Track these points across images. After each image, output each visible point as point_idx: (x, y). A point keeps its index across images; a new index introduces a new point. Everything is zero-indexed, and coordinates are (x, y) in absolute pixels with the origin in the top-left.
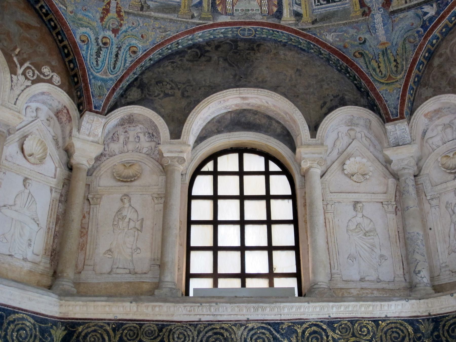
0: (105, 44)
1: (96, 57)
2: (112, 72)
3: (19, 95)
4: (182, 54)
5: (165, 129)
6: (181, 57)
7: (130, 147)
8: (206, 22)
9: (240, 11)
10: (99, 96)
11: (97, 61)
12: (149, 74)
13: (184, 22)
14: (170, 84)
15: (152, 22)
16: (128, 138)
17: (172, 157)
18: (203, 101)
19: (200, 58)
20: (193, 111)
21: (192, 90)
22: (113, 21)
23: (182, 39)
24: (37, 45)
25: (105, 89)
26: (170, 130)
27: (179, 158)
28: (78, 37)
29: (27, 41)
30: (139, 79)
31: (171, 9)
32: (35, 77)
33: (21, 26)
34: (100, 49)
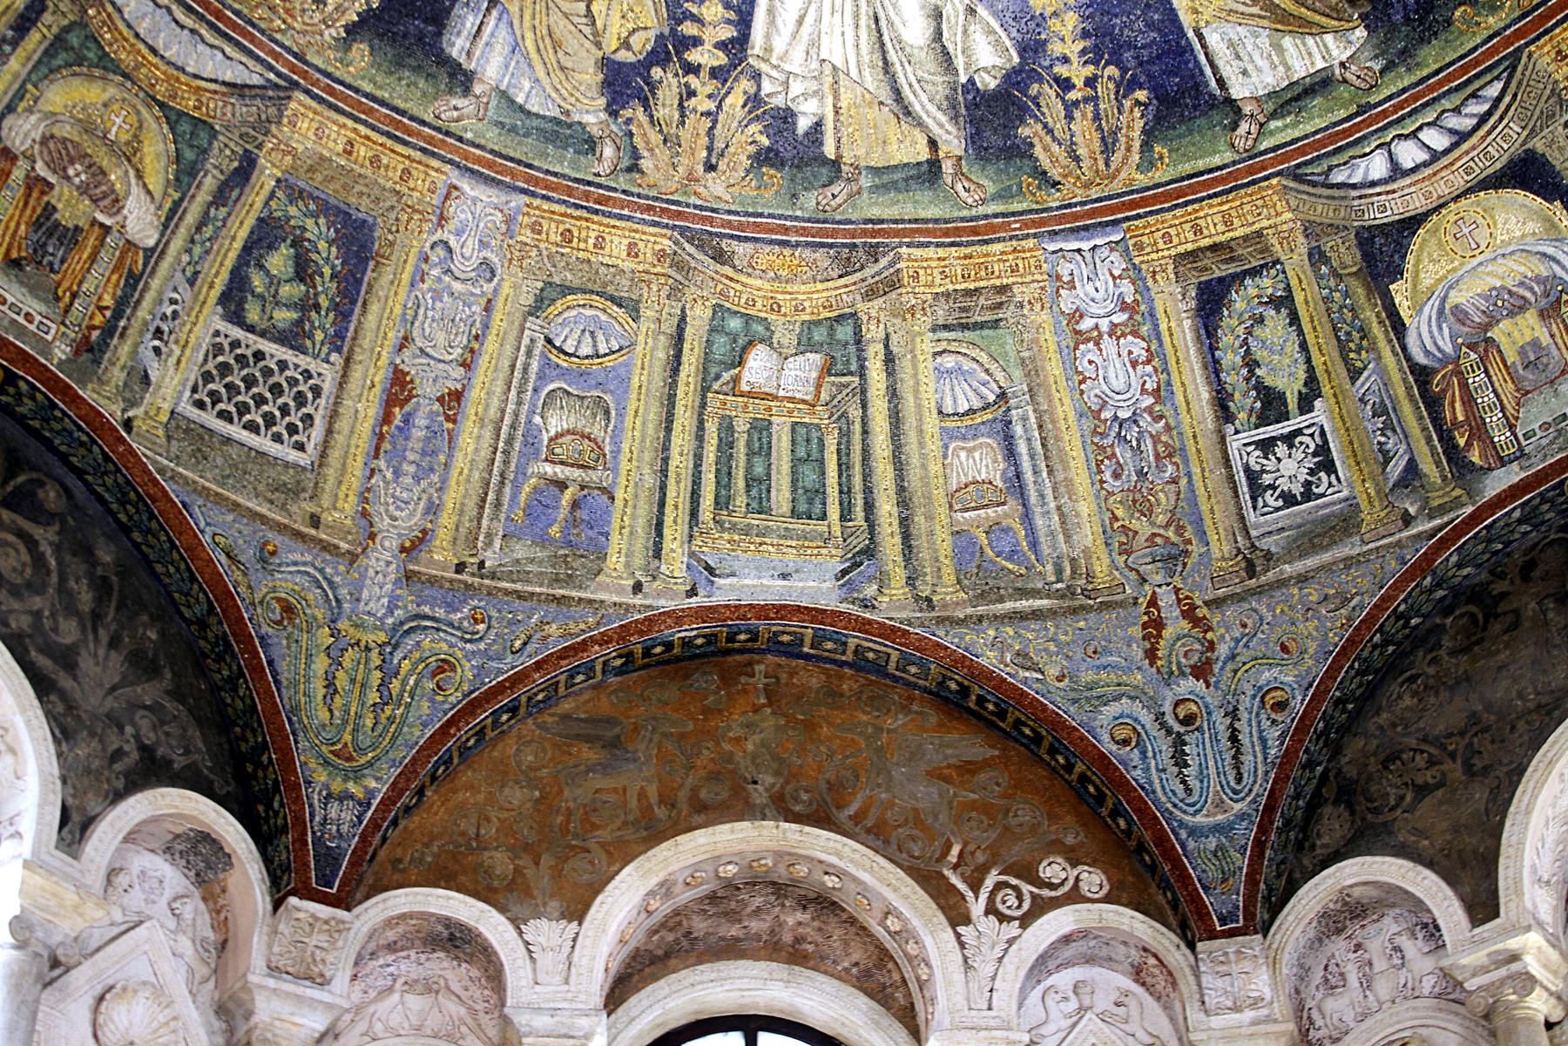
0: (1188, 720)
1: (1176, 769)
2: (1235, 792)
3: (993, 978)
4: (1433, 640)
5: (1446, 903)
6: (1431, 651)
7: (1383, 988)
8: (1452, 515)
9: (1539, 434)
10: (1224, 880)
11: (1184, 782)
12: (1355, 746)
13: (1389, 545)
14: (1422, 752)
15: (1296, 591)
16: (1370, 964)
17: (1493, 983)
18: (1534, 762)
19: (1485, 629)
20: (1512, 809)
21: (1493, 742)
22: (1183, 645)
23: (1404, 600)
24: (1008, 811)
25: (1232, 852)
26: (1462, 899)
27: (1510, 977)
28: (1106, 737)
29: (974, 814)
30: (1332, 774)
31: (1333, 528)
32: (1026, 906)
33: (947, 780)
34: (1179, 742)
